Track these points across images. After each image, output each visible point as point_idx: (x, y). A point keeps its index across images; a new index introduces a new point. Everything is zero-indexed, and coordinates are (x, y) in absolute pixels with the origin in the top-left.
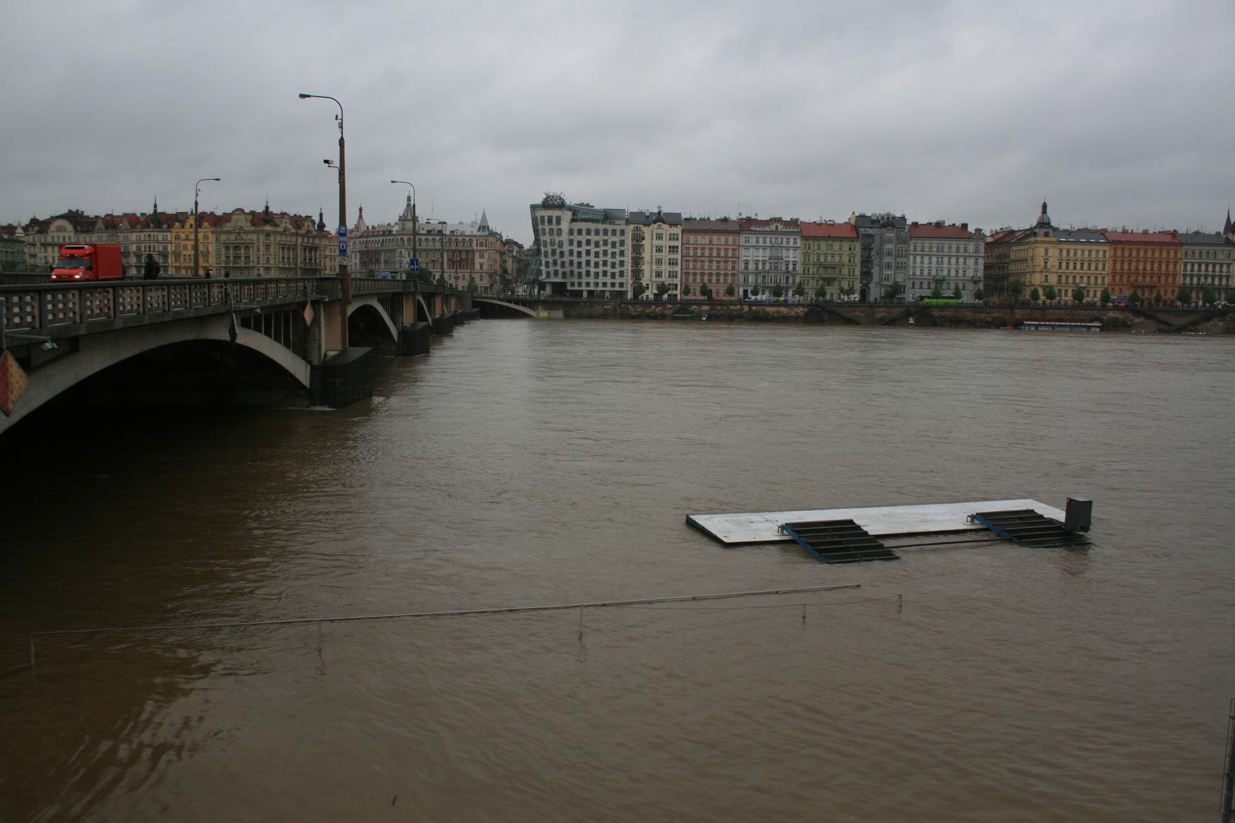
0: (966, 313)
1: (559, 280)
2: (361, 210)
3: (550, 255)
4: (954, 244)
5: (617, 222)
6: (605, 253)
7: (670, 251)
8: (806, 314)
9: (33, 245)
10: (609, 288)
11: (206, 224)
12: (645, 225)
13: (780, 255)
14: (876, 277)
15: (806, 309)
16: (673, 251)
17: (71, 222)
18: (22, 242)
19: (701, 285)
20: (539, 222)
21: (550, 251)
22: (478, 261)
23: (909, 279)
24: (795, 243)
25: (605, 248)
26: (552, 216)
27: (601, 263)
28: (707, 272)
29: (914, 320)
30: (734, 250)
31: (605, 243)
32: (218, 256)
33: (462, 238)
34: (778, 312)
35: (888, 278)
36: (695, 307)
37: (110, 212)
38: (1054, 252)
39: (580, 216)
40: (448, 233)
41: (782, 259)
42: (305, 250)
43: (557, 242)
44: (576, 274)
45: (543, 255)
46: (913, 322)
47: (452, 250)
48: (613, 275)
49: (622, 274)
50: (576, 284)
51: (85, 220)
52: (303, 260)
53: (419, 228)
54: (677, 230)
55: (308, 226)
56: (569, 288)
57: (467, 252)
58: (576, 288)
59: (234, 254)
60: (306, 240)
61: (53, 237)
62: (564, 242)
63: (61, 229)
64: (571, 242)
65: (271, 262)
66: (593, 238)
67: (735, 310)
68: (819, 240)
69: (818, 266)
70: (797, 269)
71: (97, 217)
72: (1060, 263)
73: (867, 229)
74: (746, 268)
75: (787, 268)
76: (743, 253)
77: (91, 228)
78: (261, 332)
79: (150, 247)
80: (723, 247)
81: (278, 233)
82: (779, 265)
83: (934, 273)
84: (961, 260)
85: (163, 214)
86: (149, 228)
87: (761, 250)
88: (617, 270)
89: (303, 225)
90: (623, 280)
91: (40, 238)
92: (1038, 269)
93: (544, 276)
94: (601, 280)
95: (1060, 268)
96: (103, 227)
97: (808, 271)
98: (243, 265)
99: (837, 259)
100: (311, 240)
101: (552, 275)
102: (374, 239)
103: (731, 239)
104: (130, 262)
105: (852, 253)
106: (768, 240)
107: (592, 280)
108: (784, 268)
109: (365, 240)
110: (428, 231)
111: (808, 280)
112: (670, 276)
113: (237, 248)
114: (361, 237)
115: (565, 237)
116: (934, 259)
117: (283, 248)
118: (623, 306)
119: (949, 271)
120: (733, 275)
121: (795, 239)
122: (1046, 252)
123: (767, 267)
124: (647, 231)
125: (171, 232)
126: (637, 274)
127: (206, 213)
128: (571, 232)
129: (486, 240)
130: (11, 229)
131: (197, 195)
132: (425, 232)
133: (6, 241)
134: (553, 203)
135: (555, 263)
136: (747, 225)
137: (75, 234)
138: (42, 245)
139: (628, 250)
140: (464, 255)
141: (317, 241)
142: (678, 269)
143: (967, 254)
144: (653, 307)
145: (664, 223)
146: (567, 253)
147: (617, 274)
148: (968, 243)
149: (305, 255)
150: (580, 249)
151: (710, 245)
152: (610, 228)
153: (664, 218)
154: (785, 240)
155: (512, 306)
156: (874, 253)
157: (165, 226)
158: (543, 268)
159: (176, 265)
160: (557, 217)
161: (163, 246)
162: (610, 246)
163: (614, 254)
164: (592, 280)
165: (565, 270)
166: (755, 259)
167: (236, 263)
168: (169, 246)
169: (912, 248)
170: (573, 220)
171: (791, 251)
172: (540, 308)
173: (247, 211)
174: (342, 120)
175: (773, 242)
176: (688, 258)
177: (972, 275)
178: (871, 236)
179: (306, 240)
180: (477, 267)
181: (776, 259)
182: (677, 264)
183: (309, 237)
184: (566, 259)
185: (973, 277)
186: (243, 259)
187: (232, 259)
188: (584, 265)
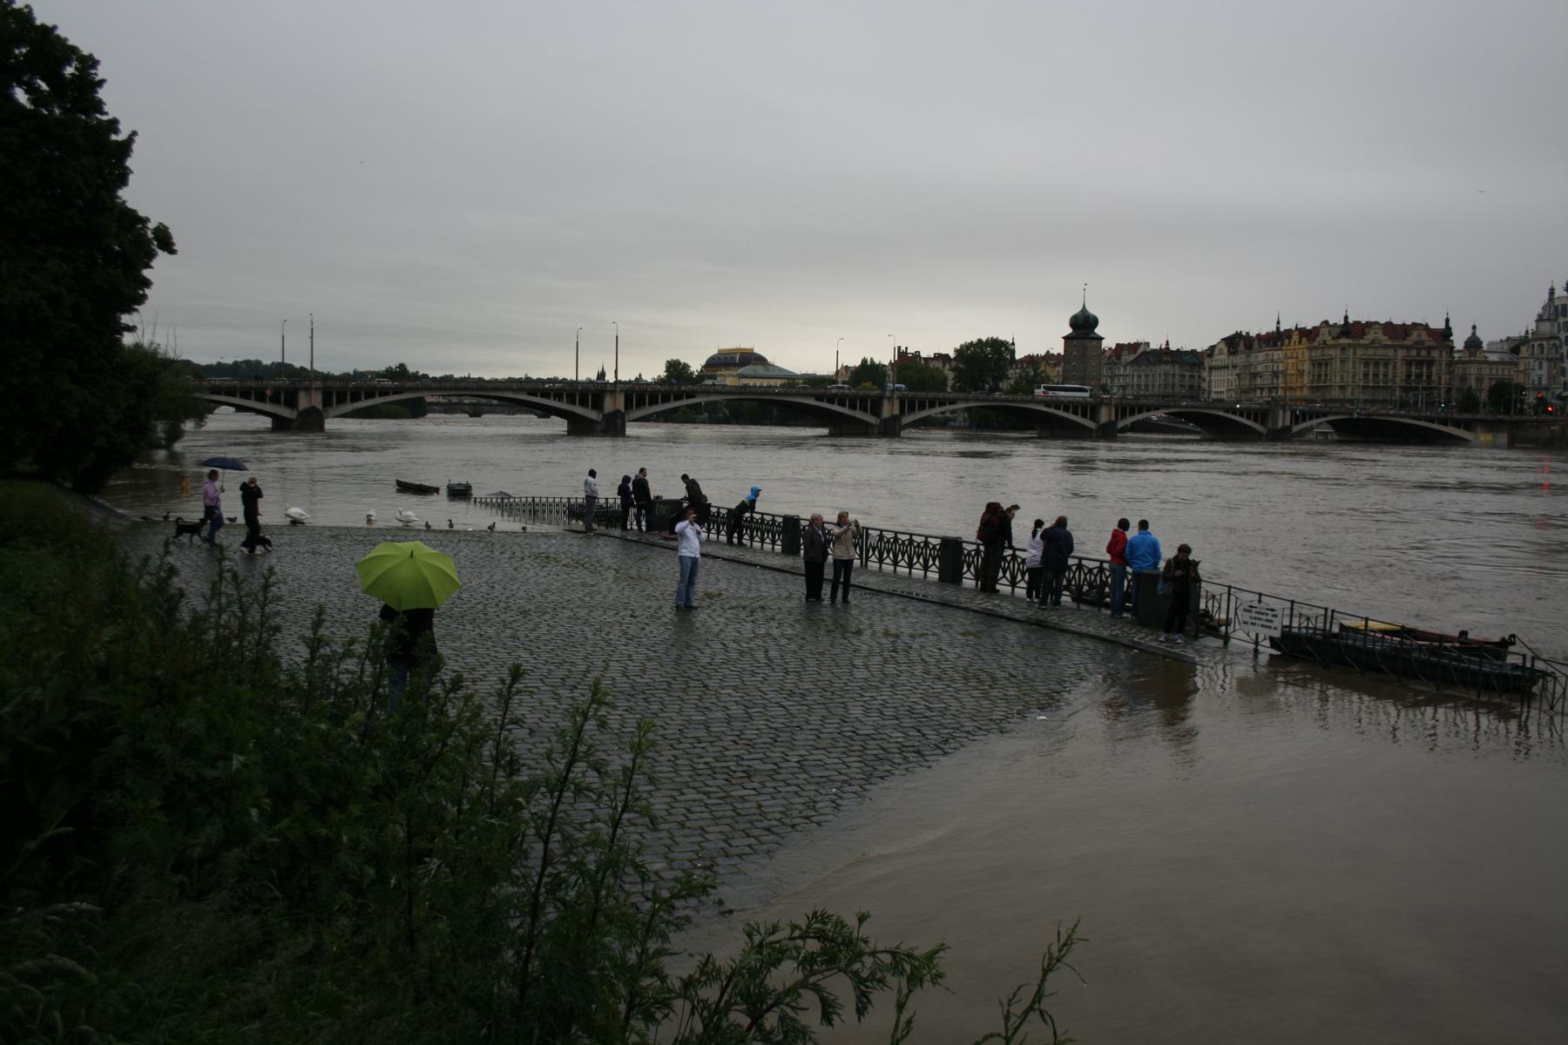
52: (1404, 377)
55: (1419, 335)
63: (1221, 353)
81: (1360, 346)
86: (1268, 345)
100: (1424, 353)
113: (1320, 365)
117: (1366, 364)
125: (1281, 350)
141: (1435, 354)
155: (1435, 426)
173: (1331, 323)
179: (1414, 353)
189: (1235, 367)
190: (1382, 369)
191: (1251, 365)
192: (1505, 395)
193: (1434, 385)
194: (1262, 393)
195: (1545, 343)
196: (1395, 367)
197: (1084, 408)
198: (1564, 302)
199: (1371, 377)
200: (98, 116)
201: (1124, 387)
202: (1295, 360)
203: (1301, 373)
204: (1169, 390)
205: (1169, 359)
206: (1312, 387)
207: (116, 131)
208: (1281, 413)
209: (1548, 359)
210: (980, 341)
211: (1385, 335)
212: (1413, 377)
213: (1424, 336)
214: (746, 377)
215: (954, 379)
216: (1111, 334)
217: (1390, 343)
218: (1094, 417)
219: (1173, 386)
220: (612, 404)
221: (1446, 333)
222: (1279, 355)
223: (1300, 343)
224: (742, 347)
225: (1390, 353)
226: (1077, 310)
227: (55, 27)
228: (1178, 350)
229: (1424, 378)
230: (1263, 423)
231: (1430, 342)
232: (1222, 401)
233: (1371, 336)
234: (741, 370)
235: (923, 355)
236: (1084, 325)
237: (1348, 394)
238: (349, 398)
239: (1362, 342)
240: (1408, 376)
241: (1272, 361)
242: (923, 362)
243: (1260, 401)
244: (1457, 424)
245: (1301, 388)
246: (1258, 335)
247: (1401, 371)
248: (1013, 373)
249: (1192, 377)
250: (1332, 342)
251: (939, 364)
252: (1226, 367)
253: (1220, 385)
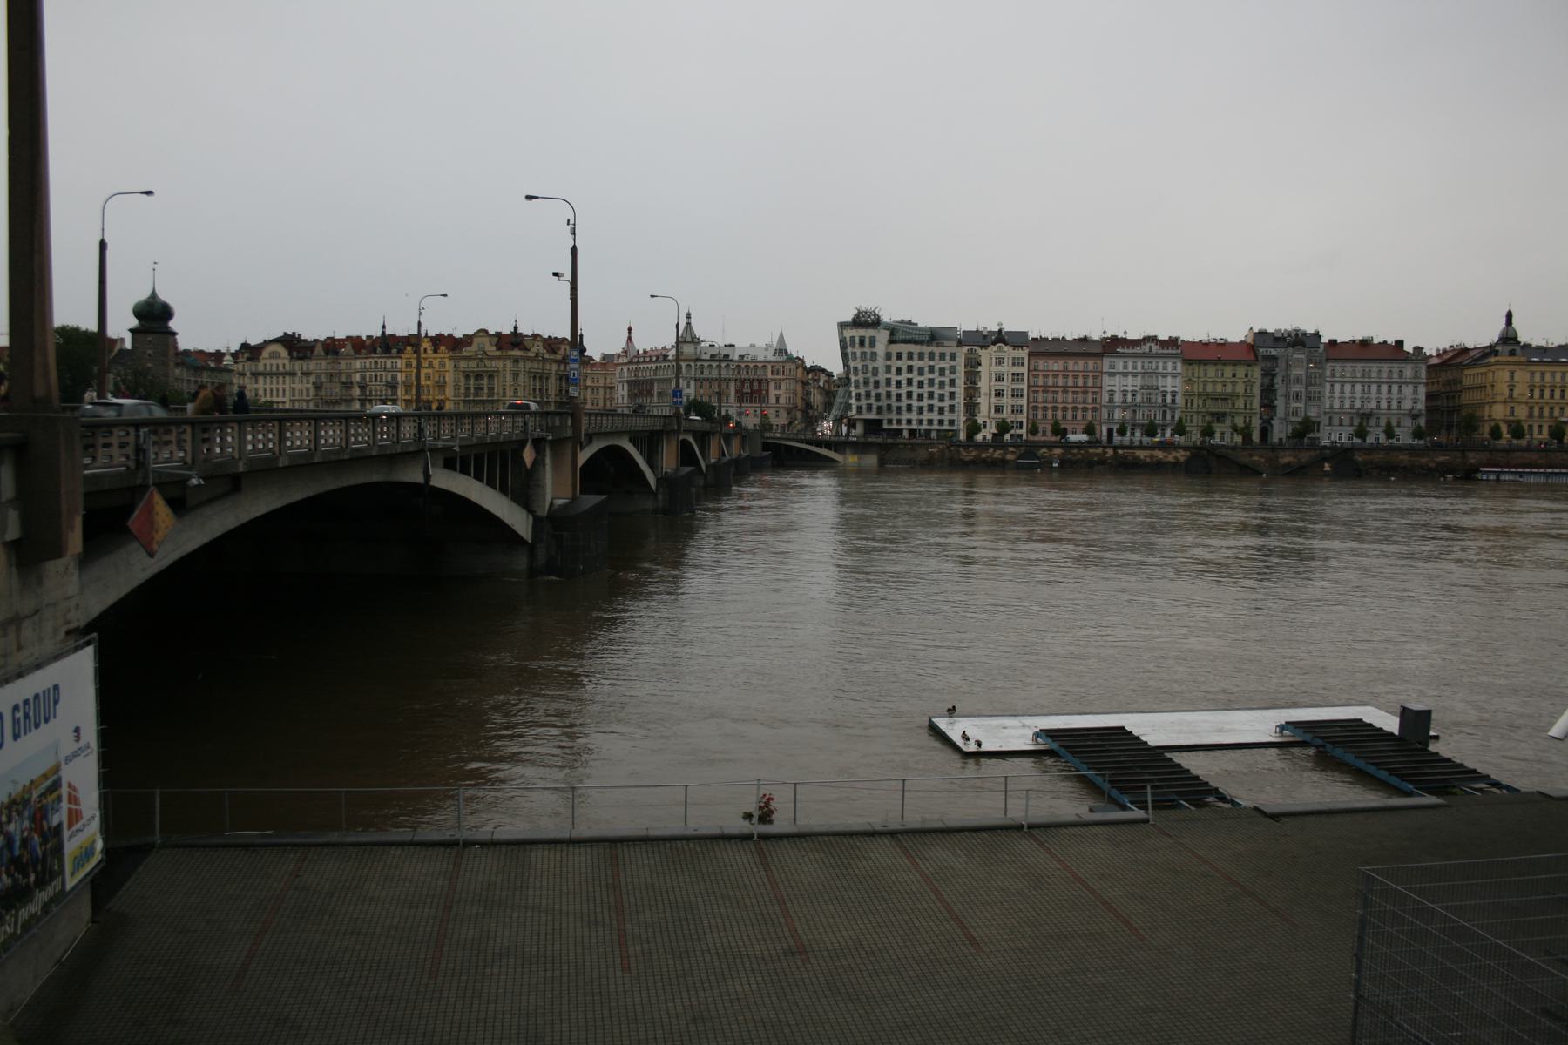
0: (1401, 457)
1: (873, 416)
2: (630, 330)
3: (861, 385)
4: (1386, 366)
5: (946, 343)
6: (931, 382)
7: (1013, 380)
8: (1188, 461)
9: (242, 374)
10: (935, 426)
11: (443, 348)
12: (982, 347)
13: (1155, 383)
14: (1280, 412)
15: (1188, 453)
16: (1018, 380)
17: (285, 347)
18: (231, 371)
19: (1052, 422)
20: (848, 344)
21: (861, 381)
22: (773, 392)
23: (1325, 413)
24: (1174, 368)
25: (931, 376)
26: (864, 337)
27: (926, 395)
28: (1061, 406)
29: (1330, 467)
30: (1095, 377)
31: (931, 369)
32: (457, 387)
33: (754, 364)
34: (1152, 456)
35: (1297, 412)
36: (1044, 450)
37: (331, 335)
38: (1522, 376)
39: (899, 336)
40: (736, 358)
41: (1157, 389)
42: (561, 379)
43: (870, 369)
44: (894, 408)
45: (853, 385)
46: (1329, 469)
47: (741, 379)
48: (941, 410)
49: (952, 409)
50: (894, 422)
51: (303, 344)
53: (700, 352)
54: (1023, 353)
56: (886, 426)
57: (760, 381)
58: (895, 426)
59: (475, 384)
60: (562, 367)
61: (265, 365)
62: (880, 370)
63: (274, 355)
64: (888, 369)
65: (519, 395)
66: (916, 363)
67: (1097, 454)
68: (1205, 364)
69: (1204, 398)
70: (1177, 401)
71: (316, 341)
72: (1532, 391)
73: (1269, 350)
74: (1111, 400)
75: (1164, 400)
76: (1108, 383)
77: (309, 354)
78: (469, 475)
79: (376, 376)
80: (1081, 374)
81: (528, 358)
82: (1154, 397)
83: (1358, 404)
84: (1395, 388)
85: (393, 336)
86: (375, 353)
87: (1130, 378)
88: (946, 404)
89: (560, 348)
90: (953, 416)
91: (249, 367)
92: (1500, 398)
93: (854, 411)
94: (926, 416)
95: (1532, 397)
96: (322, 353)
97: (1192, 404)
98: (485, 398)
99: (1229, 389)
101: (864, 410)
102: (645, 366)
103: (1091, 364)
104: (353, 394)
105: (1249, 381)
106: (1139, 365)
107: (914, 416)
108: (1160, 400)
109: (634, 367)
110: (712, 356)
111: (1191, 416)
112: (1013, 411)
113: (478, 377)
114: (630, 362)
115: (880, 363)
116: (1358, 387)
117: (534, 378)
118: (952, 449)
119: (1379, 402)
120: (1094, 409)
121: (1175, 363)
122: (1512, 377)
123: (1138, 399)
124: (984, 355)
125: (401, 358)
126: (971, 408)
127: (443, 335)
128: (888, 356)
129: (784, 367)
130: (218, 355)
131: (420, 314)
132: (708, 357)
133: (212, 370)
134: (865, 321)
135: (868, 395)
136: (1113, 345)
137: (290, 362)
138: (253, 374)
139: (960, 379)
140: (755, 385)
142: (1024, 402)
143: (1403, 381)
144: (991, 450)
145: (1006, 344)
146: (882, 383)
147: (947, 409)
148: (1404, 365)
149: (561, 386)
150: (899, 378)
151: (1064, 371)
152: (937, 350)
153: (1006, 337)
154: (1161, 365)
156: (1278, 380)
157: (394, 351)
158: (853, 401)
159: (407, 397)
160: (871, 337)
161: (392, 375)
162: (937, 374)
163: (942, 384)
164: (914, 416)
165: (880, 404)
166: (1123, 388)
167: (478, 396)
168: (399, 374)
169: (1328, 373)
170: (892, 342)
171: (1169, 379)
172: (848, 451)
173: (492, 332)
174: (574, 224)
175: (1146, 367)
176: (1037, 389)
177: (1410, 407)
178: (1274, 358)
179: (562, 367)
180: (772, 400)
181: (1150, 389)
182: (1022, 396)
184: (882, 390)
185: (1410, 410)
186: (486, 391)
187: (472, 391)
188: (904, 397)
189: (307, 374)
191: (340, 373)
195: (692, 364)
202: (445, 367)
209: (695, 380)
223: (435, 351)
226: (143, 295)
241: (385, 369)
252: (293, 374)
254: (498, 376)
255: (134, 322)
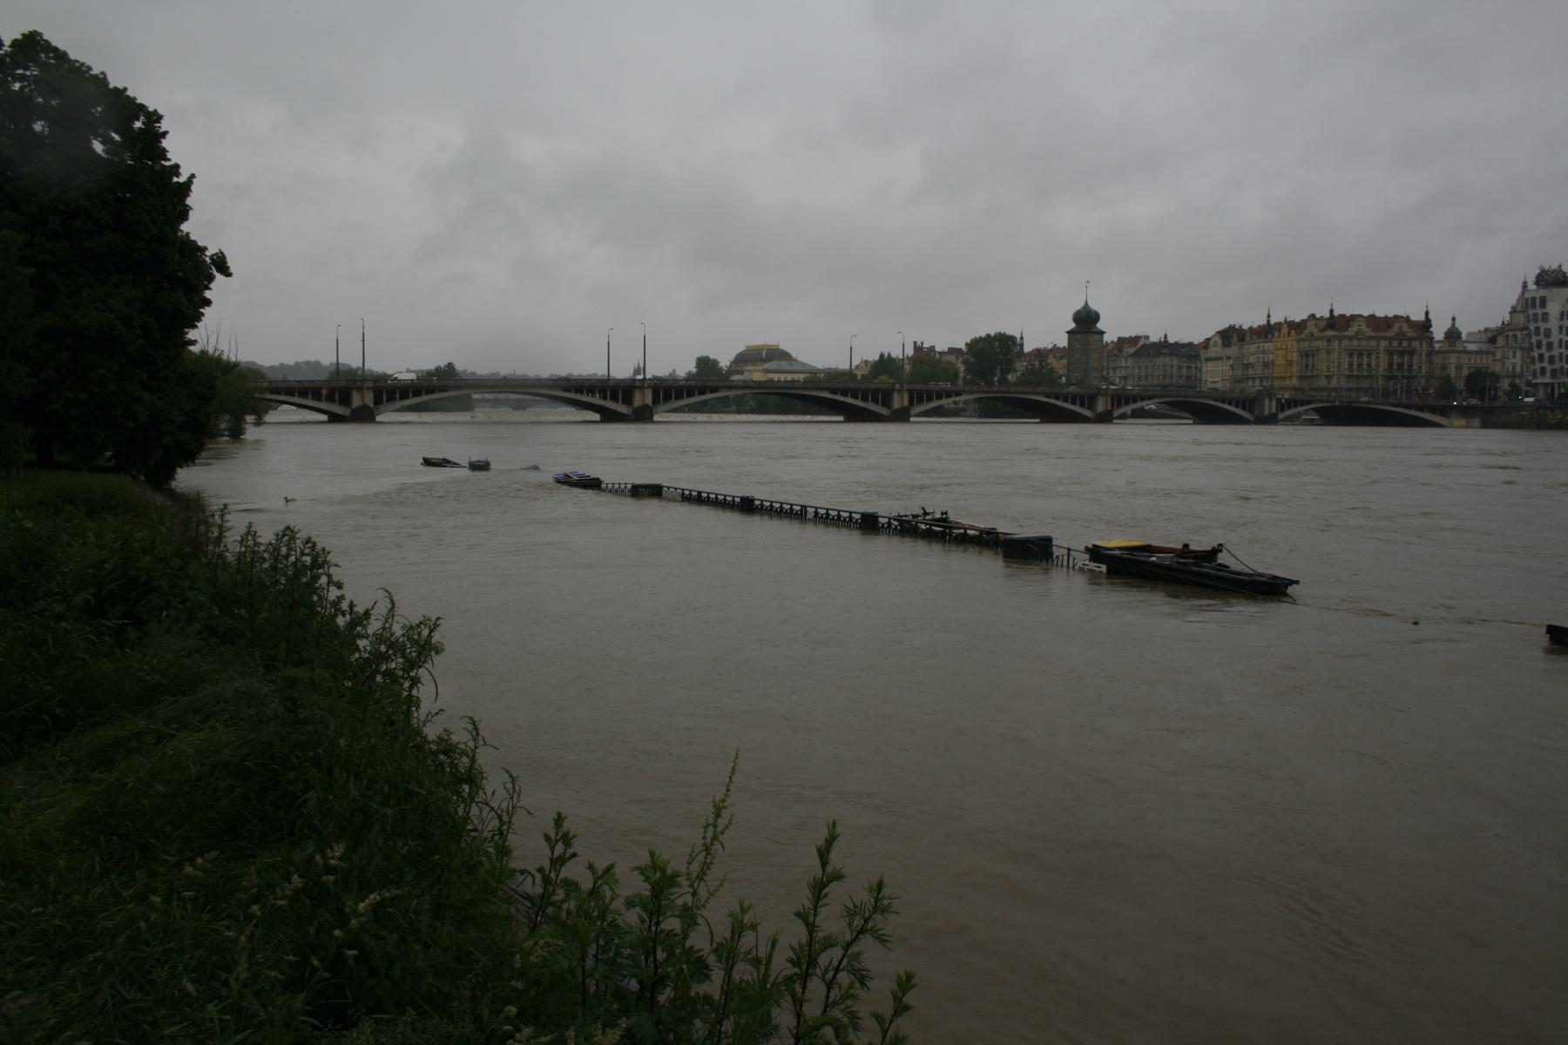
1: (1547, 380)
52: (1386, 366)
55: (1401, 327)
60: (1395, 343)
63: (1216, 344)
81: (1344, 337)
86: (1259, 338)
100: (1405, 344)
101: (1539, 374)
113: (1307, 355)
115: (1553, 323)
117: (1351, 355)
118: (1540, 411)
141: (1416, 344)
146: (1556, 345)
155: (1413, 413)
160: (1541, 297)
173: (1318, 316)
179: (1395, 343)
183: (1400, 341)
184: (1556, 352)
189: (1229, 358)
190: (1365, 359)
191: (1243, 356)
192: (1479, 382)
193: (1414, 374)
194: (1254, 382)
195: (1518, 334)
196: (1378, 357)
197: (1082, 398)
198: (1533, 295)
199: (1355, 367)
200: (163, 162)
201: (1125, 378)
202: (1282, 352)
203: (1290, 364)
204: (1167, 380)
205: (1167, 351)
206: (1301, 377)
207: (178, 175)
208: (1267, 401)
209: (1521, 349)
210: (988, 336)
211: (1368, 327)
212: (1395, 367)
213: (1405, 328)
214: (771, 372)
215: (964, 372)
216: (1112, 328)
217: (1373, 334)
218: (1091, 407)
219: (1172, 376)
220: (643, 398)
221: (1426, 325)
222: (1269, 346)
224: (769, 343)
225: (1373, 343)
226: (1079, 306)
227: (125, 89)
228: (1176, 343)
229: (1406, 367)
230: (1251, 411)
231: (1410, 333)
232: (1217, 390)
233: (1355, 328)
234: (767, 366)
235: (938, 349)
236: (1086, 321)
237: (1334, 383)
238: (398, 396)
239: (1347, 333)
240: (1390, 365)
241: (1263, 352)
242: (937, 356)
243: (1253, 390)
244: (1433, 410)
245: (1290, 377)
246: (1250, 328)
247: (1384, 360)
248: (1020, 366)
249: (1189, 367)
250: (1319, 334)
251: (952, 358)
252: (1221, 358)
253: (1215, 375)
254: (1318, 354)
255: (1072, 325)
